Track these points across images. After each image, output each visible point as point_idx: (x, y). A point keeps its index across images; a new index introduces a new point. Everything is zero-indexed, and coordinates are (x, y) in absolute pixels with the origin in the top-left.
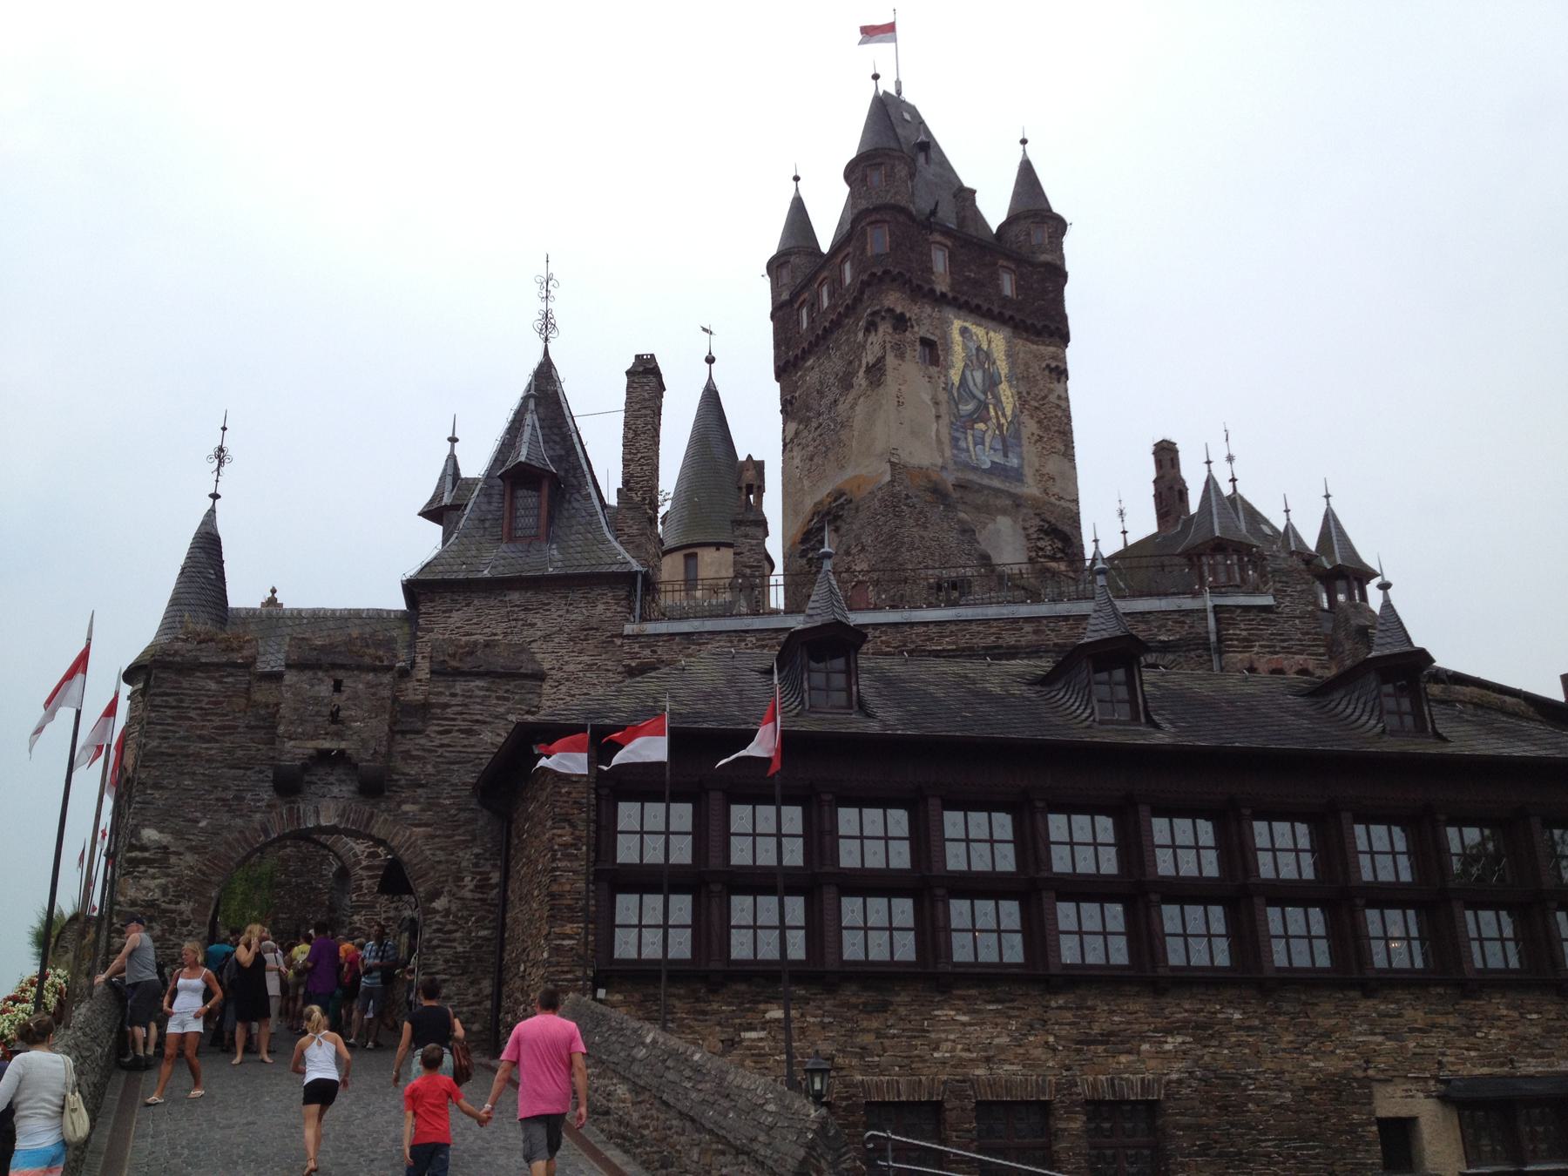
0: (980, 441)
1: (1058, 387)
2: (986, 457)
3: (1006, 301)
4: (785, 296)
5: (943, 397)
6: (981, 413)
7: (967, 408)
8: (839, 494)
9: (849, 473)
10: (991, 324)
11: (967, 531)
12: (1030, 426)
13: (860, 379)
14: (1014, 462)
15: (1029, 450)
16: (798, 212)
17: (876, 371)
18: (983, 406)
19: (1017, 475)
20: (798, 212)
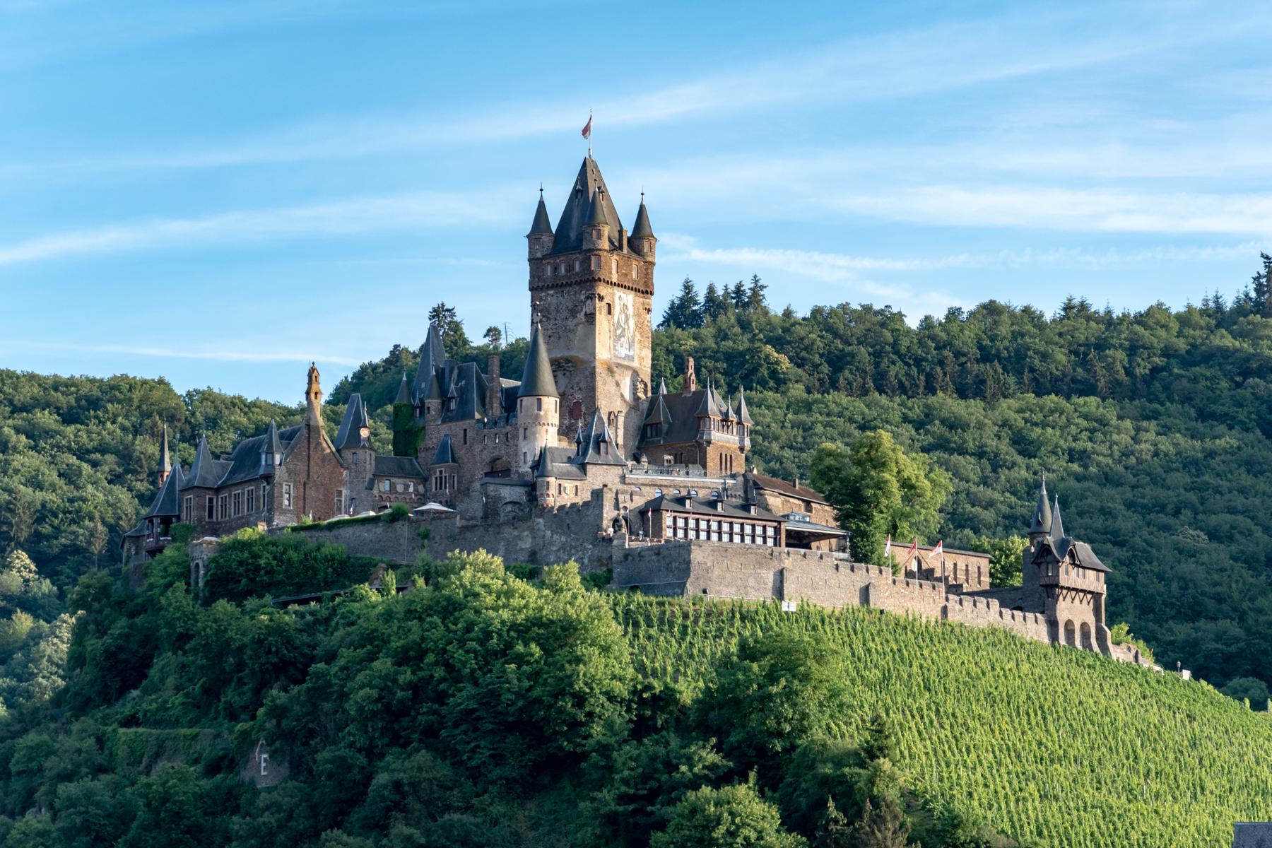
0: (622, 346)
1: (648, 316)
2: (623, 352)
3: (633, 280)
4: (539, 255)
5: (612, 328)
6: (622, 335)
7: (619, 332)
8: (568, 360)
9: (573, 353)
10: (628, 291)
11: (618, 385)
12: (638, 336)
13: (581, 316)
14: (631, 353)
15: (637, 347)
16: (541, 206)
17: (591, 318)
18: (624, 329)
19: (631, 358)
20: (541, 206)
